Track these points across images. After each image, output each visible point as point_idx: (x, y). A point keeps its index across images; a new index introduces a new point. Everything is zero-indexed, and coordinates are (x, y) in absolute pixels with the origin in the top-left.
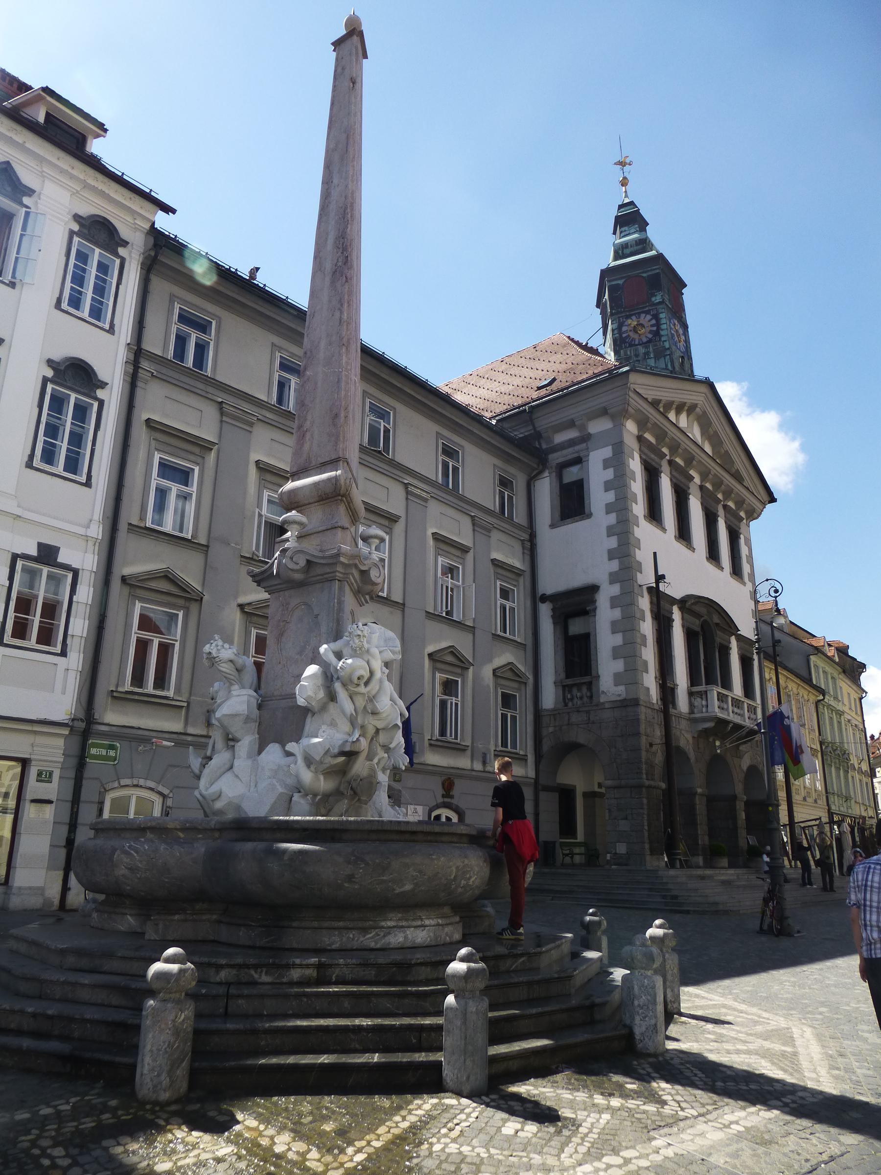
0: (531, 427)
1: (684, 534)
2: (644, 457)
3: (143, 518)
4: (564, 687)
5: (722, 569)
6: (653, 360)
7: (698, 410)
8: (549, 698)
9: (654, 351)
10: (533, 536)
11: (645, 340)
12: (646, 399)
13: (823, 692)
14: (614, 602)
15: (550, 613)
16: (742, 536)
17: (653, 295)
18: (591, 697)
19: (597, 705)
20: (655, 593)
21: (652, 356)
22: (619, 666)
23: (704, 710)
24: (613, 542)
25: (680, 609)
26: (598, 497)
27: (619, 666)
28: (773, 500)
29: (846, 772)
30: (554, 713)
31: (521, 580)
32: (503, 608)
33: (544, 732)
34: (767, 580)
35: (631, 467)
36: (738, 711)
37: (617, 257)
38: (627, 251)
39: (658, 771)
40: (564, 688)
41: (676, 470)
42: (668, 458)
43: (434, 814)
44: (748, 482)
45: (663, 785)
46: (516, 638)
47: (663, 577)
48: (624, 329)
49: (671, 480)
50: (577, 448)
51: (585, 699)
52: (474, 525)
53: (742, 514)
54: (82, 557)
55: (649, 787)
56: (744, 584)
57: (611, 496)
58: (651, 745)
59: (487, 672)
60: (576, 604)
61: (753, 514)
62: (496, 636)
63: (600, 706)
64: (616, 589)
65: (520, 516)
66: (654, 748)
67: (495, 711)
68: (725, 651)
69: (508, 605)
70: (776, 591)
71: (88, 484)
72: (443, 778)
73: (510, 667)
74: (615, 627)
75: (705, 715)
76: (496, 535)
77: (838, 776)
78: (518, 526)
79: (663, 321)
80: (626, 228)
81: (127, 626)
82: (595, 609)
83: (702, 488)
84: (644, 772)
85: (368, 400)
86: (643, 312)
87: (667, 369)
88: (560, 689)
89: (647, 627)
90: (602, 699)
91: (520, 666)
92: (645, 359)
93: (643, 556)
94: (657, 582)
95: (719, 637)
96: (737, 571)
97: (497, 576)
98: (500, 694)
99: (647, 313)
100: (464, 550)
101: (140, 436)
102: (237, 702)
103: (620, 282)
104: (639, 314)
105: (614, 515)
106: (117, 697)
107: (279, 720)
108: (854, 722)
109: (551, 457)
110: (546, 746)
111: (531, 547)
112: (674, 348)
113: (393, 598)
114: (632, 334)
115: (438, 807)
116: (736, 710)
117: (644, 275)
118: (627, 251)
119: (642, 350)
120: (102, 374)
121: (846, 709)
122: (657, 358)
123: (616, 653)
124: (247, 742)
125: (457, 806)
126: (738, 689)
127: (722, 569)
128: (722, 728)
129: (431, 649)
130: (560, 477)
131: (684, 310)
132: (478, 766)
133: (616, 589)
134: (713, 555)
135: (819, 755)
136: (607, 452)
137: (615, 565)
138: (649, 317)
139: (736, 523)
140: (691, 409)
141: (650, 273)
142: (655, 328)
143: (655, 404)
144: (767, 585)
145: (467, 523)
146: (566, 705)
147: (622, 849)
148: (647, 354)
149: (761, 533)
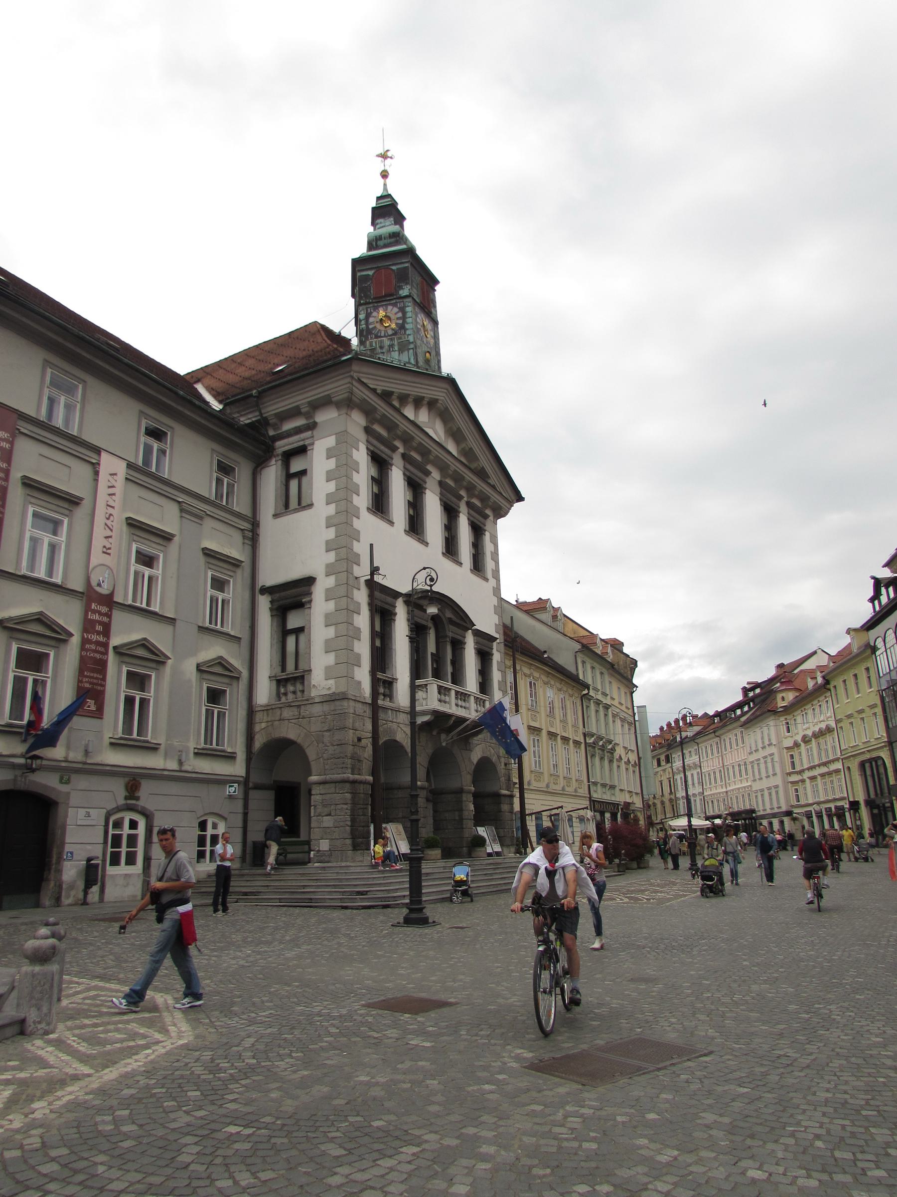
0: (257, 413)
1: (415, 526)
2: (372, 448)
4: (279, 682)
5: (460, 564)
6: (397, 353)
7: (439, 405)
8: (264, 693)
9: (399, 343)
10: (255, 525)
11: (390, 332)
12: (374, 391)
13: (587, 687)
14: (329, 595)
15: (269, 605)
16: (487, 534)
17: (401, 288)
18: (303, 691)
19: (307, 700)
20: (371, 584)
21: (396, 348)
22: (331, 659)
23: (424, 702)
24: (331, 534)
25: (407, 603)
26: (320, 486)
27: (331, 659)
28: (520, 499)
29: (611, 761)
30: (268, 709)
31: (239, 571)
32: (214, 600)
33: (257, 728)
34: (424, 569)
35: (354, 457)
36: (464, 704)
37: (371, 245)
39: (367, 765)
40: (280, 682)
41: (410, 464)
42: (401, 450)
43: (112, 820)
44: (493, 480)
45: (370, 778)
47: (377, 569)
48: (371, 320)
49: (404, 474)
50: (303, 436)
51: (299, 694)
52: (182, 510)
53: (488, 512)
55: (354, 782)
56: (487, 580)
57: (331, 487)
58: (359, 739)
59: (189, 667)
60: (291, 597)
61: (500, 512)
62: (202, 629)
63: (310, 702)
64: (331, 581)
65: (241, 504)
66: (364, 742)
67: (198, 706)
68: (458, 646)
69: (221, 596)
70: (432, 580)
72: (127, 779)
73: (220, 662)
74: (329, 621)
75: (424, 708)
76: (209, 523)
77: (602, 767)
78: (238, 515)
79: (409, 315)
80: (381, 220)
82: (310, 602)
83: (441, 483)
84: (349, 766)
85: (49, 371)
86: (390, 304)
87: (409, 363)
88: (274, 683)
89: (363, 620)
90: (314, 693)
91: (232, 661)
92: (389, 351)
93: (361, 548)
94: (372, 574)
95: (451, 632)
96: (478, 566)
97: (208, 565)
98: (205, 689)
99: (395, 305)
100: (167, 537)
103: (371, 273)
104: (386, 305)
105: (333, 505)
108: (622, 715)
109: (278, 444)
110: (258, 744)
111: (252, 536)
112: (418, 342)
113: (71, 586)
114: (378, 326)
115: (119, 809)
116: (460, 703)
117: (394, 268)
118: (381, 243)
119: (387, 342)
121: (616, 703)
122: (401, 351)
123: (329, 647)
125: (143, 808)
126: (471, 682)
127: (460, 564)
128: (441, 722)
130: (286, 464)
131: (435, 307)
132: (173, 765)
133: (331, 581)
134: (450, 549)
135: (583, 746)
136: (331, 441)
137: (331, 557)
138: (396, 310)
139: (481, 519)
140: (432, 404)
141: (400, 266)
142: (400, 322)
143: (386, 396)
144: (424, 574)
145: (172, 510)
146: (279, 698)
147: (324, 845)
148: (392, 346)
149: (510, 532)
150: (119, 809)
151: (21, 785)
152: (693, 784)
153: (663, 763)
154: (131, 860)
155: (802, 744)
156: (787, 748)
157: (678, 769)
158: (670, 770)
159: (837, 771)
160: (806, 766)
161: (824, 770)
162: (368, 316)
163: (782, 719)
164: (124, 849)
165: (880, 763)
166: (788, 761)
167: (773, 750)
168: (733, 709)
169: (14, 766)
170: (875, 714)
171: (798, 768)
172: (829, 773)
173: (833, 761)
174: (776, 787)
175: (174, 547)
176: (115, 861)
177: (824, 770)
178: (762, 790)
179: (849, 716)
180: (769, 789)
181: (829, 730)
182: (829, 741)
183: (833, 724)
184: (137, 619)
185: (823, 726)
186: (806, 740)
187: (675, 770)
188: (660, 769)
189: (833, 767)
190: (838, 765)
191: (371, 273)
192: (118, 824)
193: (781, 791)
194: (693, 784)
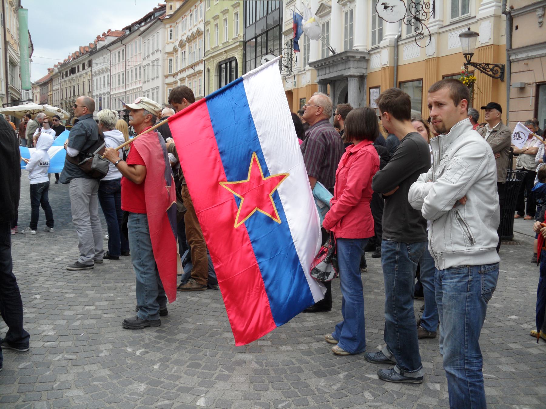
152: (104, 84)
153: (86, 67)
155: (180, 49)
156: (169, 53)
157: (95, 73)
158: (90, 72)
159: (200, 72)
160: (179, 69)
161: (191, 71)
163: (168, 26)
165: (234, 64)
166: (167, 63)
167: (159, 55)
168: (139, 23)
170: (236, 14)
171: (174, 71)
172: (194, 75)
173: (197, 64)
174: (158, 88)
177: (191, 71)
178: (148, 91)
179: (216, 18)
180: (153, 89)
181: (199, 33)
182: (198, 44)
183: (202, 27)
185: (195, 30)
186: (182, 45)
187: (93, 73)
188: (84, 71)
189: (197, 69)
190: (201, 67)
193: (160, 90)
194: (104, 84)
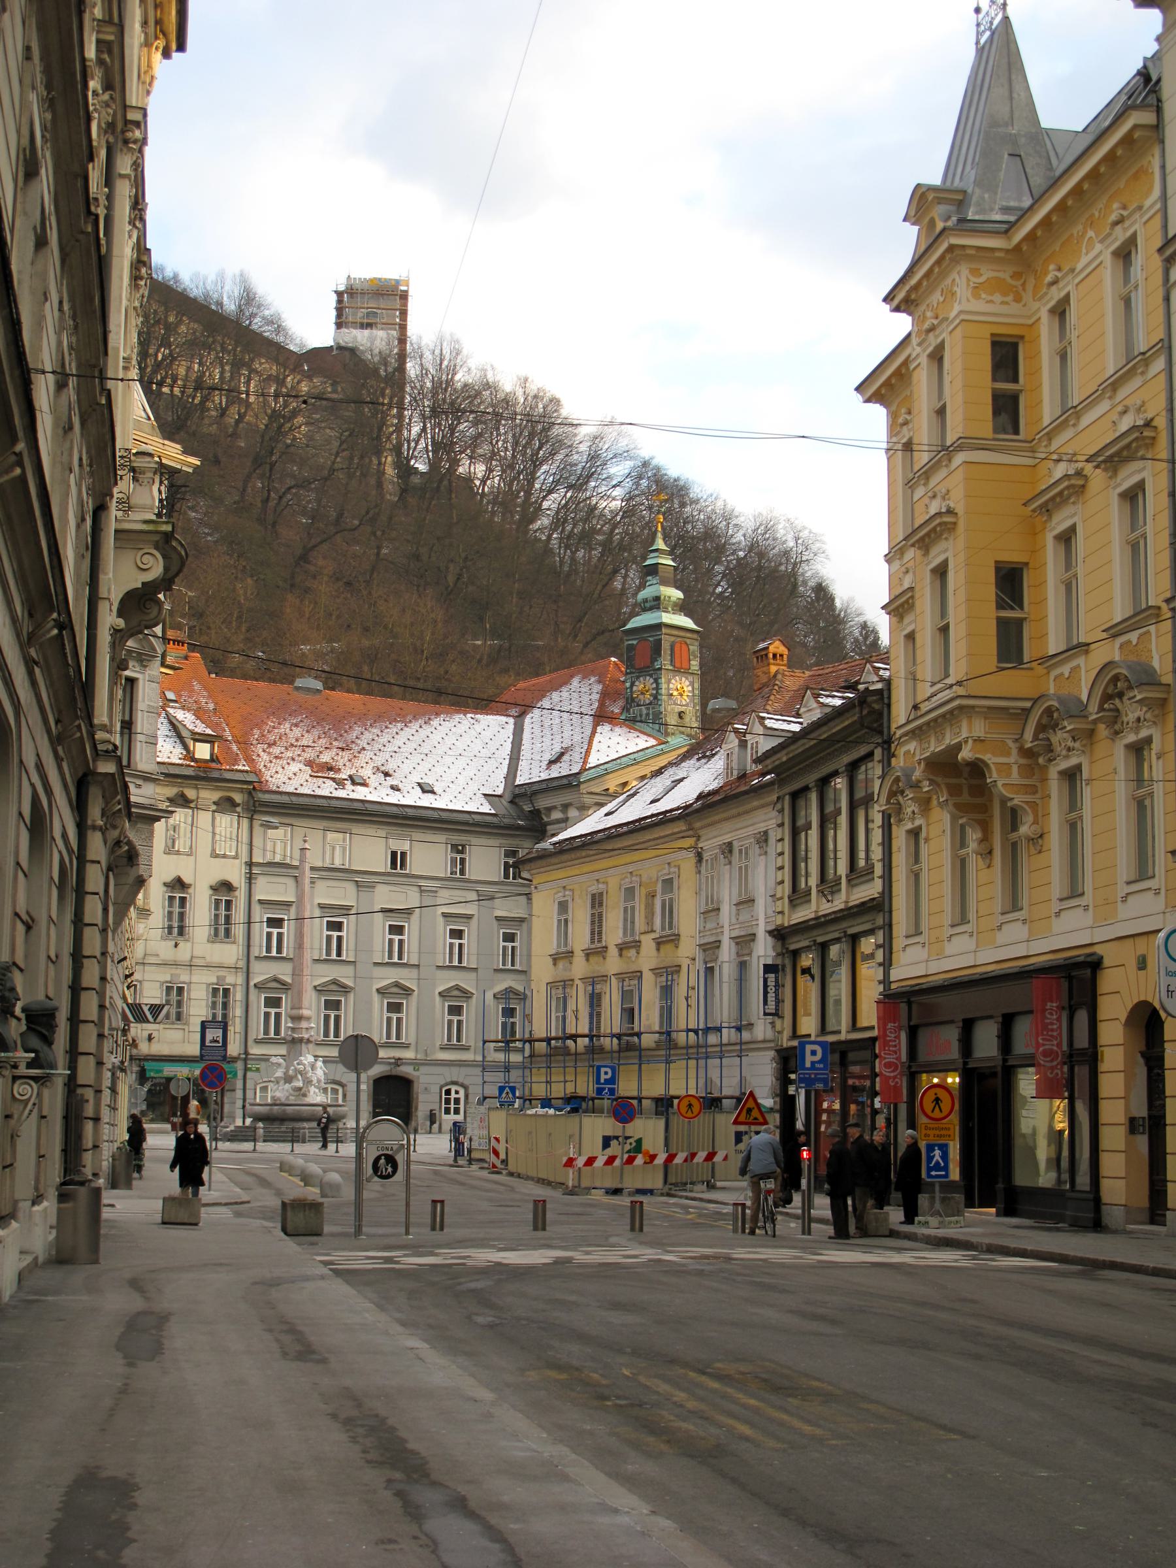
3: (261, 951)
38: (647, 605)
46: (517, 967)
48: (635, 688)
54: (234, 980)
59: (489, 996)
71: (234, 943)
81: (259, 1007)
99: (651, 676)
100: (469, 917)
101: (257, 909)
102: (279, 1073)
103: (635, 642)
106: (258, 1042)
107: (288, 1079)
115: (447, 1084)
120: (235, 884)
124: (282, 1082)
129: (441, 989)
148: (648, 714)
150: (447, 1084)
151: (394, 1073)
154: (457, 1111)
162: (632, 684)
164: (452, 1106)
169: (390, 1064)
175: (474, 921)
176: (447, 1111)
184: (453, 973)
191: (635, 642)
192: (448, 1092)
